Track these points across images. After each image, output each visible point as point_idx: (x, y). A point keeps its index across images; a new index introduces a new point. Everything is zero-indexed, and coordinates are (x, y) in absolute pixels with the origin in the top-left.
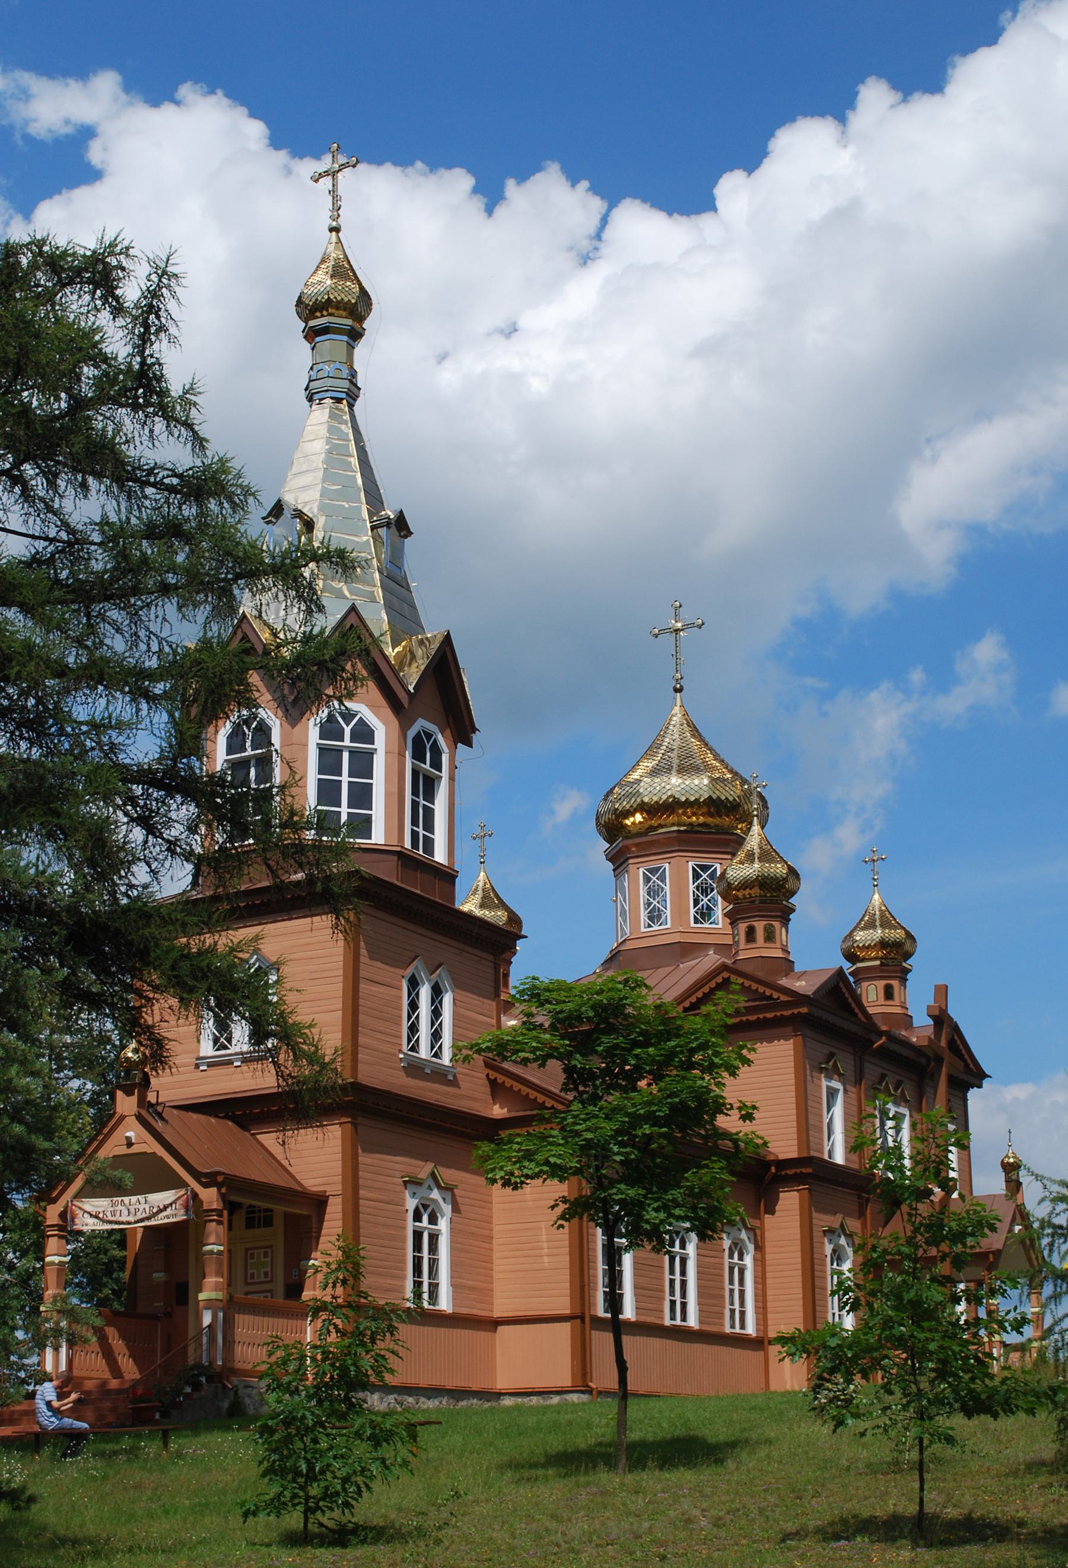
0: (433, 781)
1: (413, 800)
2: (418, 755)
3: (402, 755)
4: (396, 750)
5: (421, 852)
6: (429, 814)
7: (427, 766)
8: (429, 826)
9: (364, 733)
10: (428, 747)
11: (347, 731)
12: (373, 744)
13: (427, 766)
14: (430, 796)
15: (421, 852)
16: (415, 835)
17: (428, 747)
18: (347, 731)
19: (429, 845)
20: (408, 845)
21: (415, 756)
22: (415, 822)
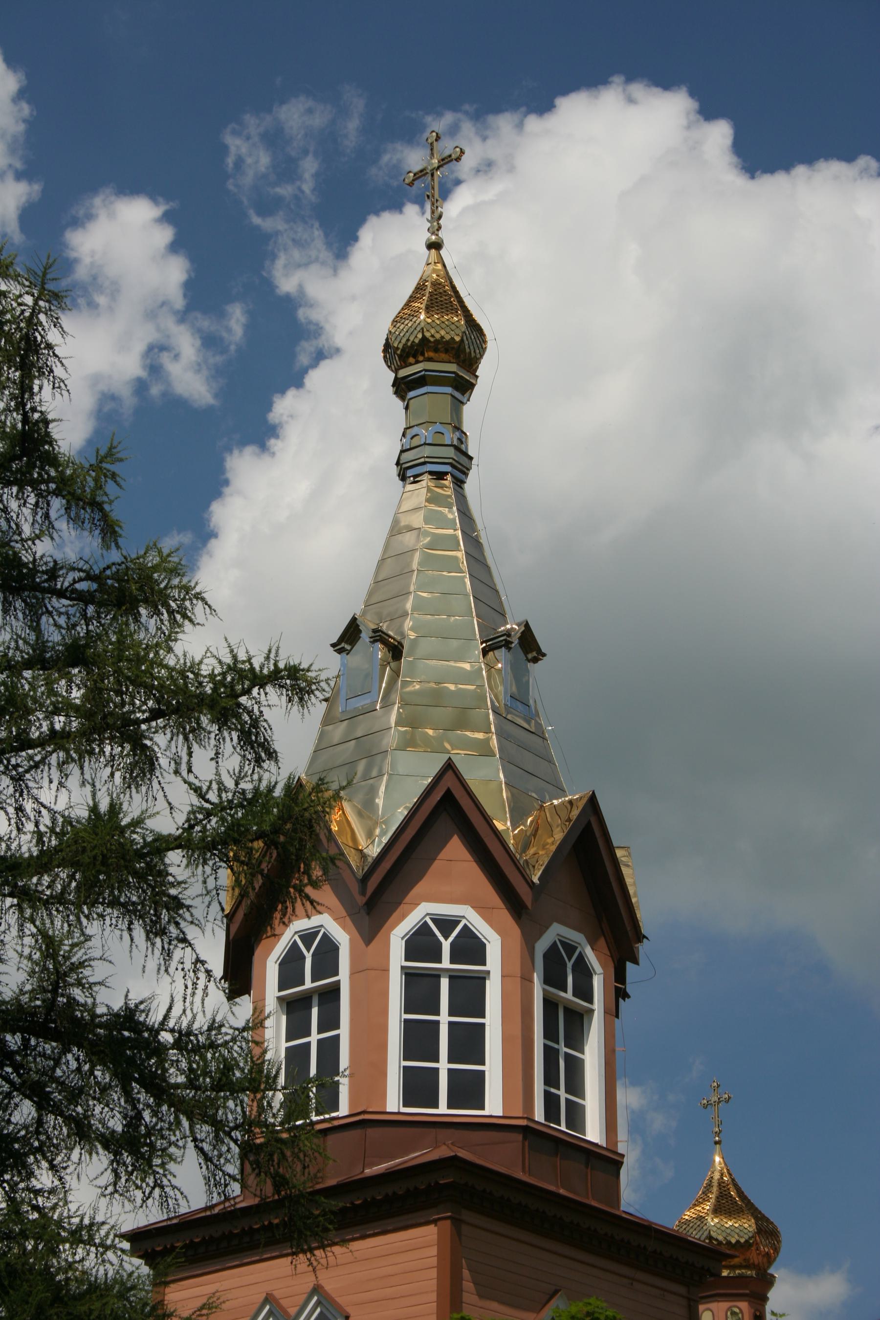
2: (554, 978)
3: (527, 979)
4: (517, 971)
5: (563, 1128)
6: (575, 1068)
7: (569, 995)
8: (576, 1085)
10: (569, 965)
11: (446, 945)
12: (484, 964)
13: (569, 995)
14: (576, 1040)
15: (563, 1128)
16: (551, 1102)
17: (569, 965)
18: (446, 945)
19: (576, 1115)
20: (539, 1115)
21: (548, 980)
22: (551, 1079)
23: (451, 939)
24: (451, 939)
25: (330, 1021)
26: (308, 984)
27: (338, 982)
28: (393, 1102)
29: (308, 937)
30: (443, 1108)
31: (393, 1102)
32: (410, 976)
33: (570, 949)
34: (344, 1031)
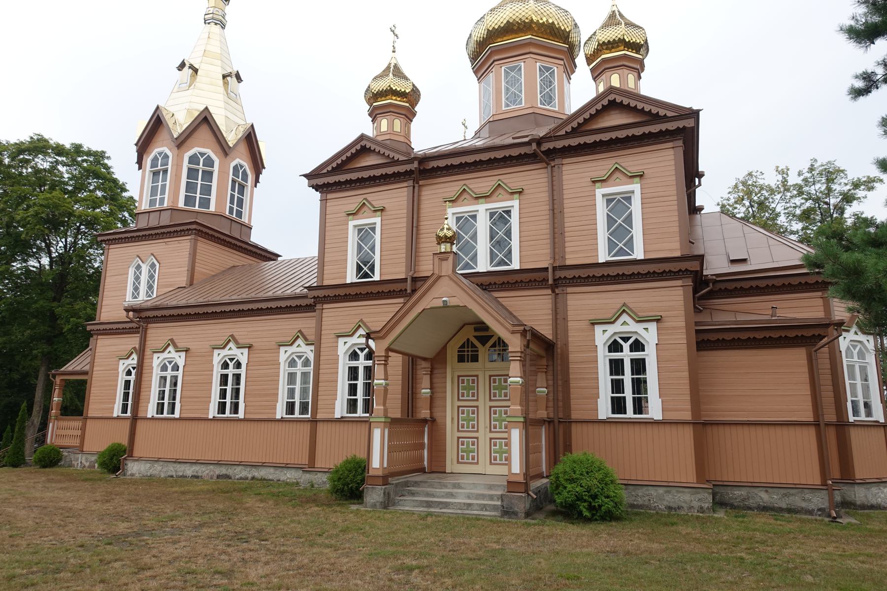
0: (244, 187)
1: (231, 194)
5: (234, 216)
7: (240, 180)
9: (209, 162)
10: (241, 172)
13: (240, 180)
17: (241, 172)
23: (204, 158)
24: (204, 158)
25: (164, 180)
26: (159, 168)
27: (168, 168)
28: (181, 204)
29: (160, 154)
30: (197, 208)
31: (181, 204)
32: (189, 169)
33: (242, 167)
34: (168, 183)
